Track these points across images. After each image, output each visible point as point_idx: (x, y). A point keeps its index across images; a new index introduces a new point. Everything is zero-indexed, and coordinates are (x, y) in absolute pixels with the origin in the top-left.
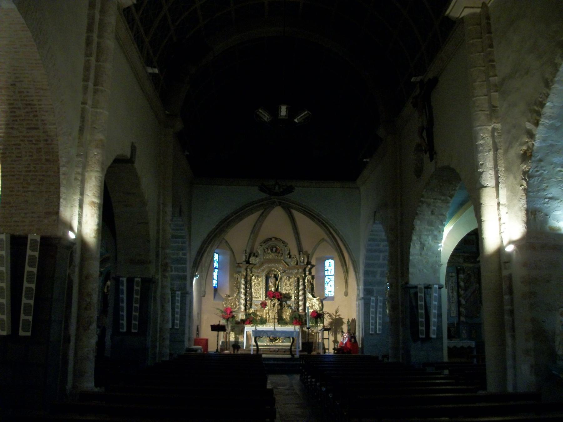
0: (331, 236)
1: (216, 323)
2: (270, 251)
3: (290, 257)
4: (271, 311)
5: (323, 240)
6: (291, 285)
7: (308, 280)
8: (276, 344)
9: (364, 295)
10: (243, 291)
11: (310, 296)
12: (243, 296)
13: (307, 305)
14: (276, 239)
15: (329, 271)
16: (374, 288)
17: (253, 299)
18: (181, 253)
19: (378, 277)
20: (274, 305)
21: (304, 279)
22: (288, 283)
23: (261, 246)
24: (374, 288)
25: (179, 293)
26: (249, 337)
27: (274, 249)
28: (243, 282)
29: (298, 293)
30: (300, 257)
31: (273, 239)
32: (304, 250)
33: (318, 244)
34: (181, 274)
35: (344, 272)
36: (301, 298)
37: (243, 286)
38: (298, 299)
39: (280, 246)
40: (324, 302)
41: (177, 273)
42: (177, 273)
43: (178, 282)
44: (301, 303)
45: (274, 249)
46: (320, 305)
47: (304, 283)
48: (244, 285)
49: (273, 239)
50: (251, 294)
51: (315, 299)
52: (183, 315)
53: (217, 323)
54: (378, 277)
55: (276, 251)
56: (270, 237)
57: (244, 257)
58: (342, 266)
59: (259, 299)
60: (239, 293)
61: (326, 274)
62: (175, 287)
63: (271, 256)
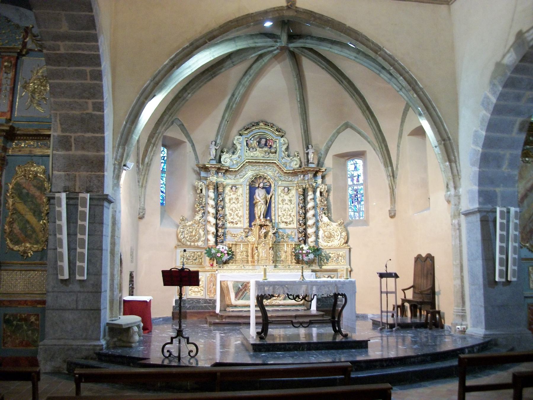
0: (367, 112)
1: (175, 263)
2: (254, 143)
3: (289, 156)
4: (262, 244)
5: (347, 126)
6: (290, 201)
7: (321, 193)
8: (274, 302)
9: (480, 203)
10: (212, 211)
11: (325, 219)
12: (213, 221)
13: (321, 233)
14: (266, 124)
15: (355, 178)
16: (498, 190)
17: (228, 225)
18: (90, 102)
19: (505, 169)
20: (266, 236)
21: (314, 192)
22: (287, 198)
23: (240, 135)
24: (498, 190)
25: (88, 196)
26: (226, 292)
27: (263, 141)
28: (212, 194)
29: (305, 214)
30: (308, 154)
31: (261, 124)
32: (313, 144)
33: (338, 132)
34: (91, 154)
35: (389, 176)
36: (310, 222)
37: (212, 203)
38: (305, 224)
39: (270, 134)
40: (350, 229)
41: (80, 153)
42: (80, 153)
43: (85, 173)
44: (310, 231)
45: (263, 141)
46: (344, 234)
47: (314, 199)
48: (214, 200)
49: (261, 124)
50: (224, 216)
51: (334, 224)
52: (96, 249)
53: (179, 266)
54: (505, 169)
55: (266, 145)
56: (256, 121)
57: (213, 152)
58: (386, 165)
59: (239, 225)
60: (205, 213)
61: (350, 182)
62: (78, 184)
63: (259, 154)
